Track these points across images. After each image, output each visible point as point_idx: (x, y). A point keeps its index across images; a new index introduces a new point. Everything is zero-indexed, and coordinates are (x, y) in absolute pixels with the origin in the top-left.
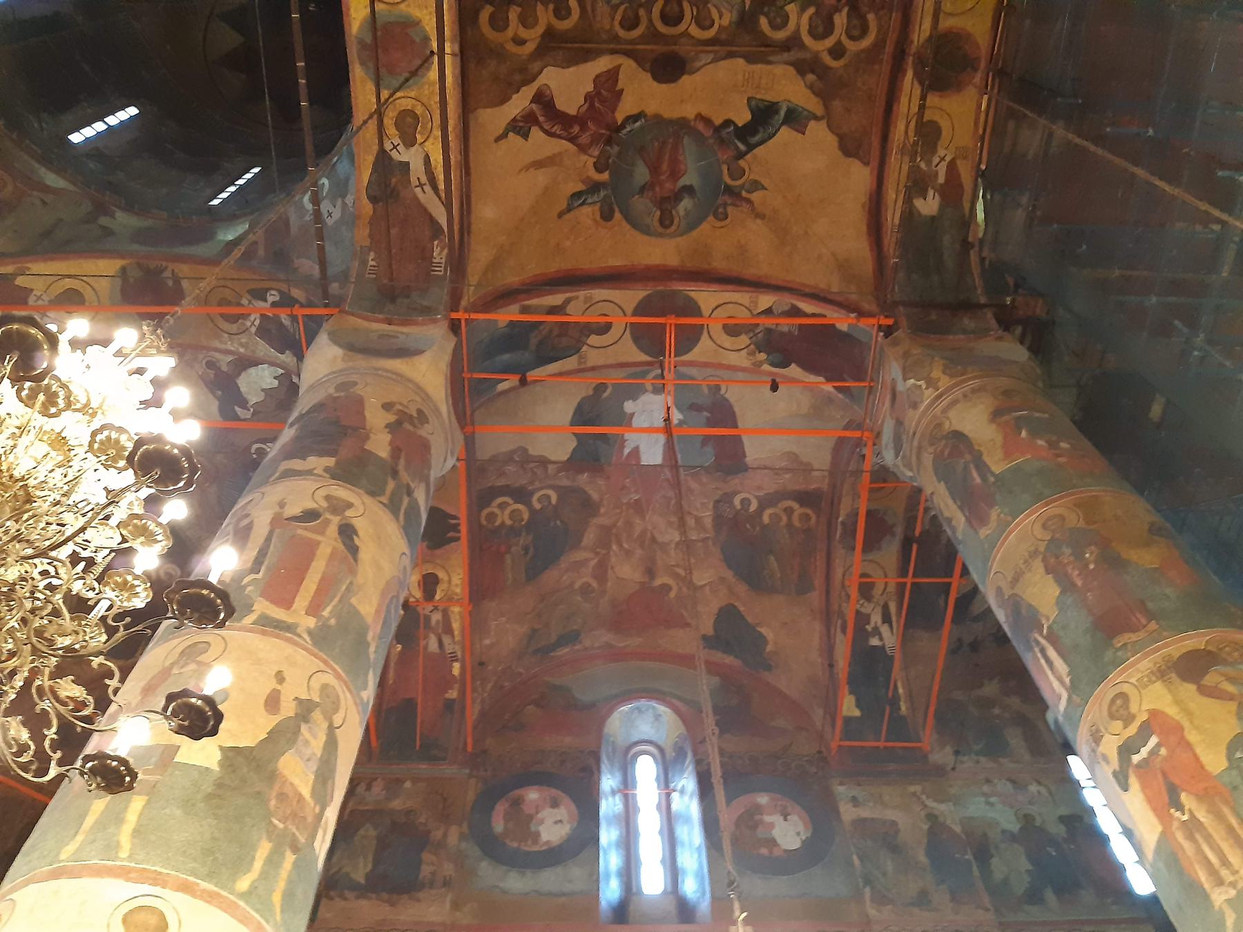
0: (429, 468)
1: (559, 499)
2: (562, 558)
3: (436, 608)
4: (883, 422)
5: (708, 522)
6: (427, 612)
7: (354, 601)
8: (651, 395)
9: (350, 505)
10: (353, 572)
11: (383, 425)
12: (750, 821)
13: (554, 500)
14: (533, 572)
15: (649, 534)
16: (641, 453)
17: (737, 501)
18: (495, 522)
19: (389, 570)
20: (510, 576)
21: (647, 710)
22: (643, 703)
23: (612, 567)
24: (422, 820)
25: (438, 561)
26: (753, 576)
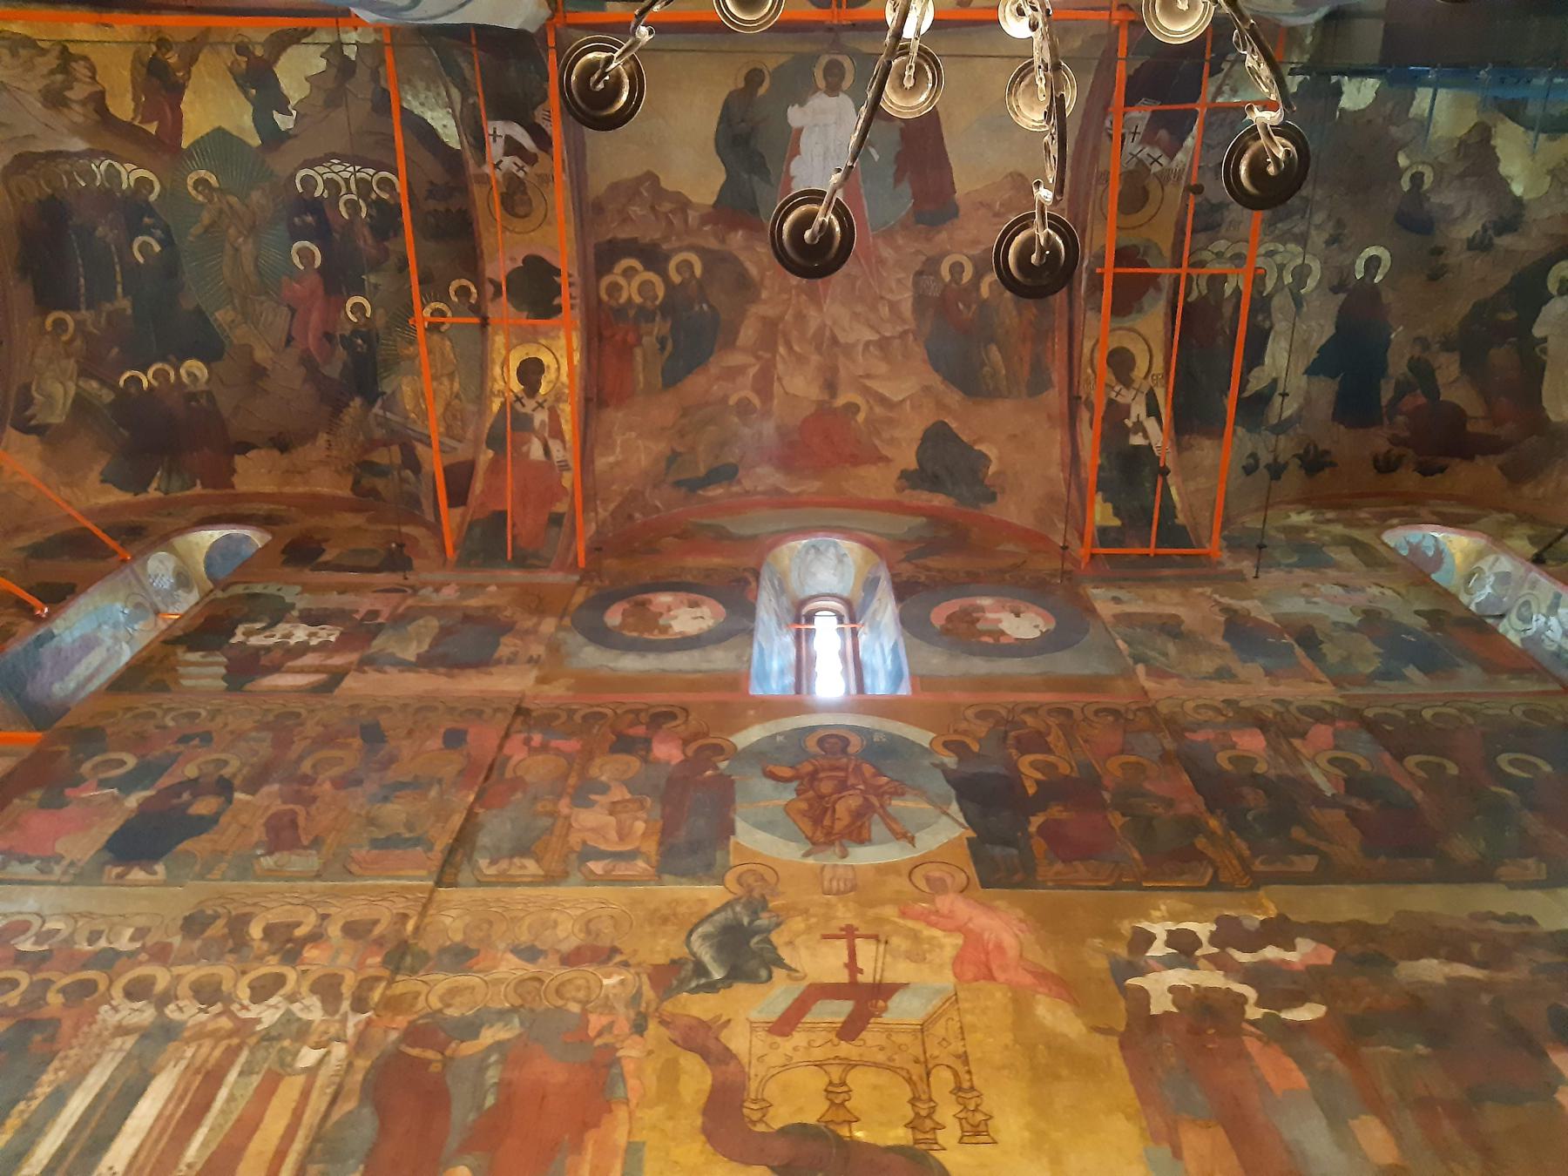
1: (706, 269)
2: (711, 359)
3: (540, 405)
5: (907, 308)
6: (528, 410)
13: (698, 271)
14: (672, 378)
15: (828, 333)
20: (641, 378)
21: (828, 547)
22: (819, 539)
23: (779, 379)
25: (543, 341)
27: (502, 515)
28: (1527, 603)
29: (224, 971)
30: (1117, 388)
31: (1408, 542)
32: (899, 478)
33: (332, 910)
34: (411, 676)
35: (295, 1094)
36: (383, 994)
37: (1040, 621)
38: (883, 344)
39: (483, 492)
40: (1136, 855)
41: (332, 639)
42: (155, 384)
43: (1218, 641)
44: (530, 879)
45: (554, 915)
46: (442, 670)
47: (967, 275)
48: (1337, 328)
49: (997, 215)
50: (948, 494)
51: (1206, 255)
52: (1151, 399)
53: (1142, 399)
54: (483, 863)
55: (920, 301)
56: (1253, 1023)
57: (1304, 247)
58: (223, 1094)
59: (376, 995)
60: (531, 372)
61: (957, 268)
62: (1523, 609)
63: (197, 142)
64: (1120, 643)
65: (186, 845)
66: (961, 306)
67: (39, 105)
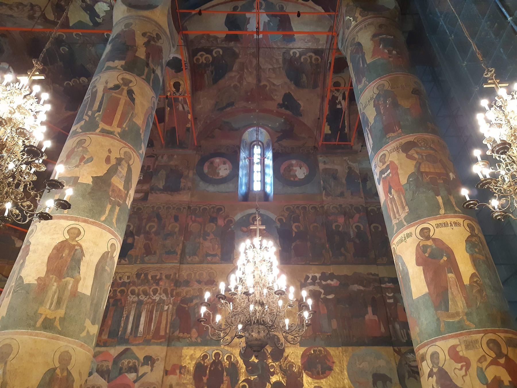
0: (162, 59)
2: (226, 75)
4: (340, 30)
5: (281, 61)
7: (134, 120)
9: (131, 81)
10: (133, 109)
11: (143, 44)
12: (289, 169)
13: (221, 53)
14: (216, 80)
18: (199, 61)
19: (147, 105)
20: (207, 83)
24: (181, 169)
26: (298, 84)
27: (174, 128)
29: (146, 287)
30: (335, 92)
32: (278, 105)
33: (162, 272)
34: (163, 195)
35: (166, 315)
36: (176, 293)
37: (305, 171)
38: (274, 70)
39: (168, 121)
40: (310, 255)
41: (142, 178)
42: (74, 84)
43: (344, 181)
44: (197, 262)
45: (202, 272)
46: (169, 192)
49: (306, 42)
50: (290, 111)
52: (344, 95)
53: (341, 95)
54: (188, 257)
55: (284, 59)
56: (322, 299)
58: (154, 316)
59: (174, 293)
60: (177, 86)
63: (74, 25)
65: (129, 253)
66: (295, 62)
67: (28, 20)
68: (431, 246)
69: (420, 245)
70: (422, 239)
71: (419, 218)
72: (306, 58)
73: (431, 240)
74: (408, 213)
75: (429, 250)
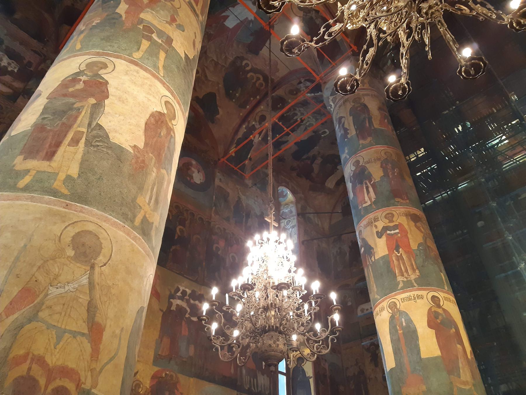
8: (251, 3)
16: (228, 19)
17: (244, 63)
28: (290, 221)
30: (257, 123)
31: (282, 190)
37: (202, 178)
38: (216, 64)
41: (16, 70)
47: (248, 68)
48: (307, 139)
51: (298, 109)
55: (233, 63)
56: (186, 318)
57: (316, 121)
61: (247, 65)
62: (288, 222)
64: (214, 196)
66: (241, 73)
68: (440, 314)
69: (431, 310)
70: (434, 305)
71: (429, 285)
72: (253, 76)
73: (441, 309)
74: (419, 276)
75: (440, 317)
